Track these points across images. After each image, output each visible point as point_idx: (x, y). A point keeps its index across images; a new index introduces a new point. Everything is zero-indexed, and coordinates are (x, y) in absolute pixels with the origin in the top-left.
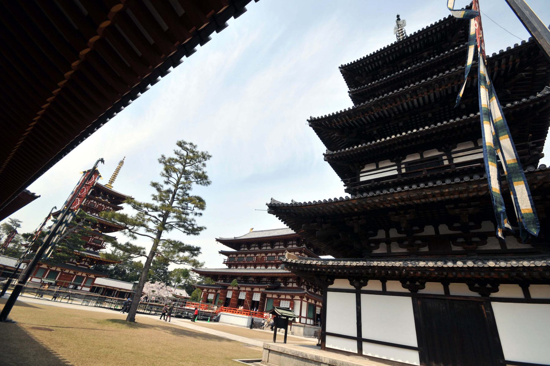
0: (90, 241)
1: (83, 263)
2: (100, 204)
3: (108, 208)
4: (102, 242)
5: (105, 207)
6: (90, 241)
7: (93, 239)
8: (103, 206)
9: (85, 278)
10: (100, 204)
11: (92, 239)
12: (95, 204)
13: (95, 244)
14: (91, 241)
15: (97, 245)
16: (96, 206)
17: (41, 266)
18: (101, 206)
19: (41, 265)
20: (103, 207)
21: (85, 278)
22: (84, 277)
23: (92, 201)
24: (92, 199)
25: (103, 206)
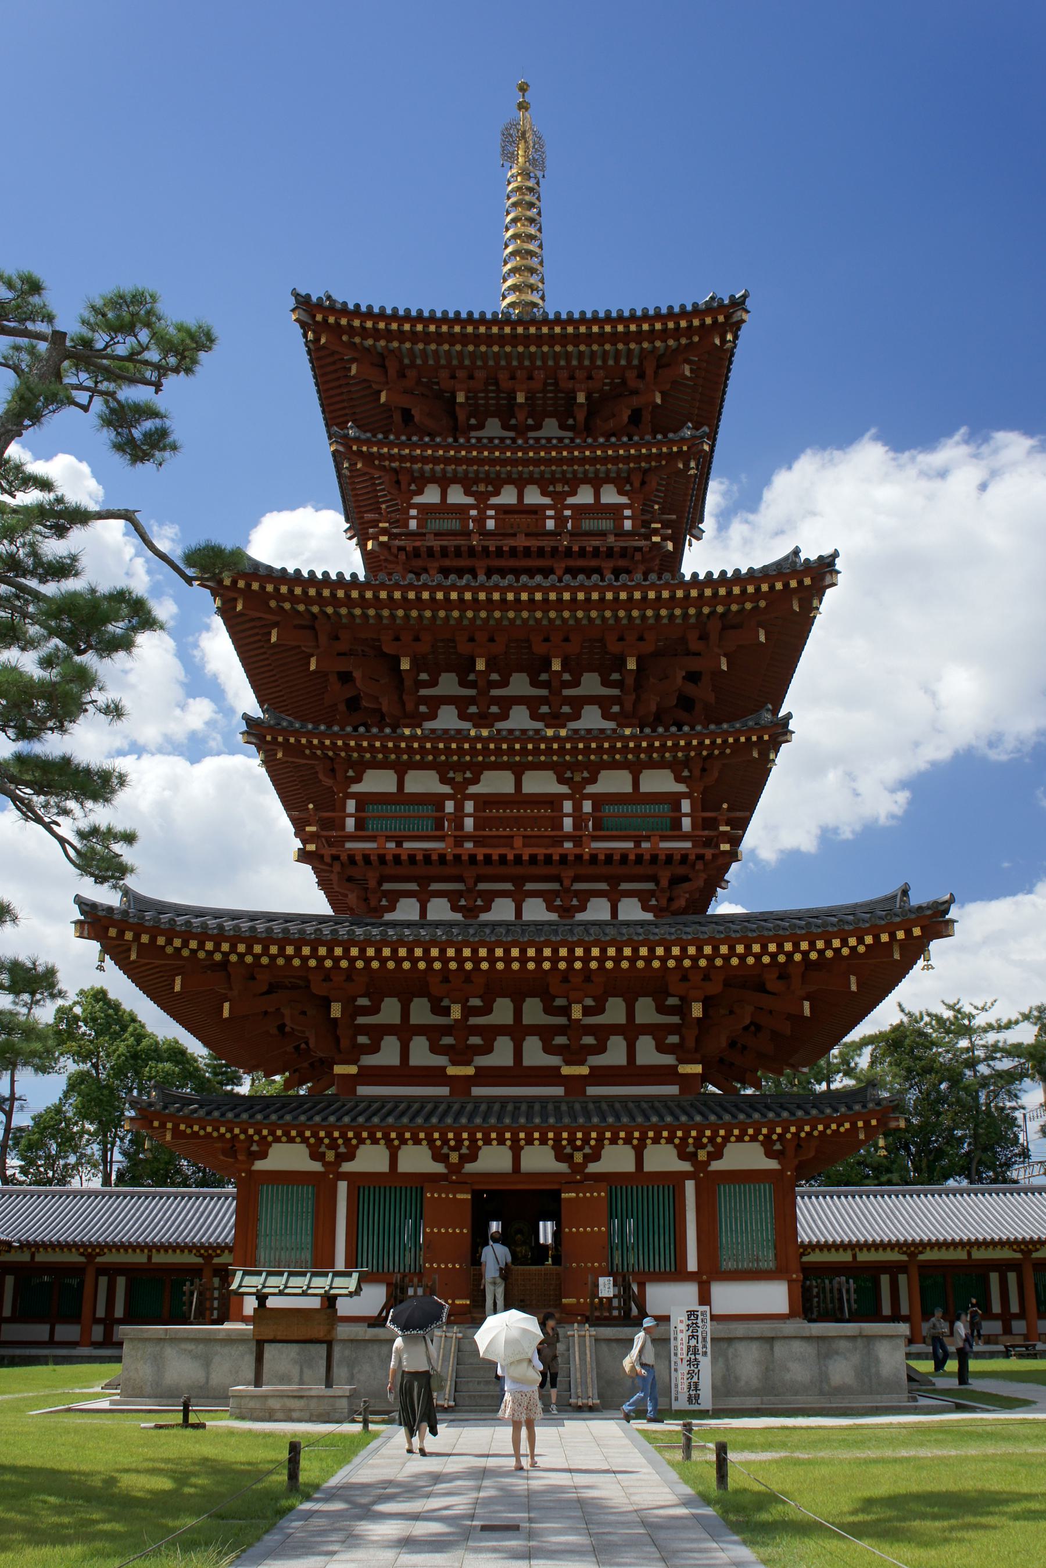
0: (568, 823)
1: (615, 1054)
2: (508, 497)
3: (584, 496)
4: (678, 807)
5: (559, 504)
6: (568, 823)
7: (587, 806)
8: (533, 497)
9: (690, 1186)
10: (508, 497)
11: (577, 807)
12: (463, 509)
13: (631, 845)
14: (576, 826)
15: (645, 845)
16: (481, 520)
17: (259, 1165)
18: (521, 509)
19: (263, 1155)
20: (537, 511)
21: (690, 1186)
22: (674, 1181)
23: (431, 496)
24: (422, 482)
25: (533, 497)
